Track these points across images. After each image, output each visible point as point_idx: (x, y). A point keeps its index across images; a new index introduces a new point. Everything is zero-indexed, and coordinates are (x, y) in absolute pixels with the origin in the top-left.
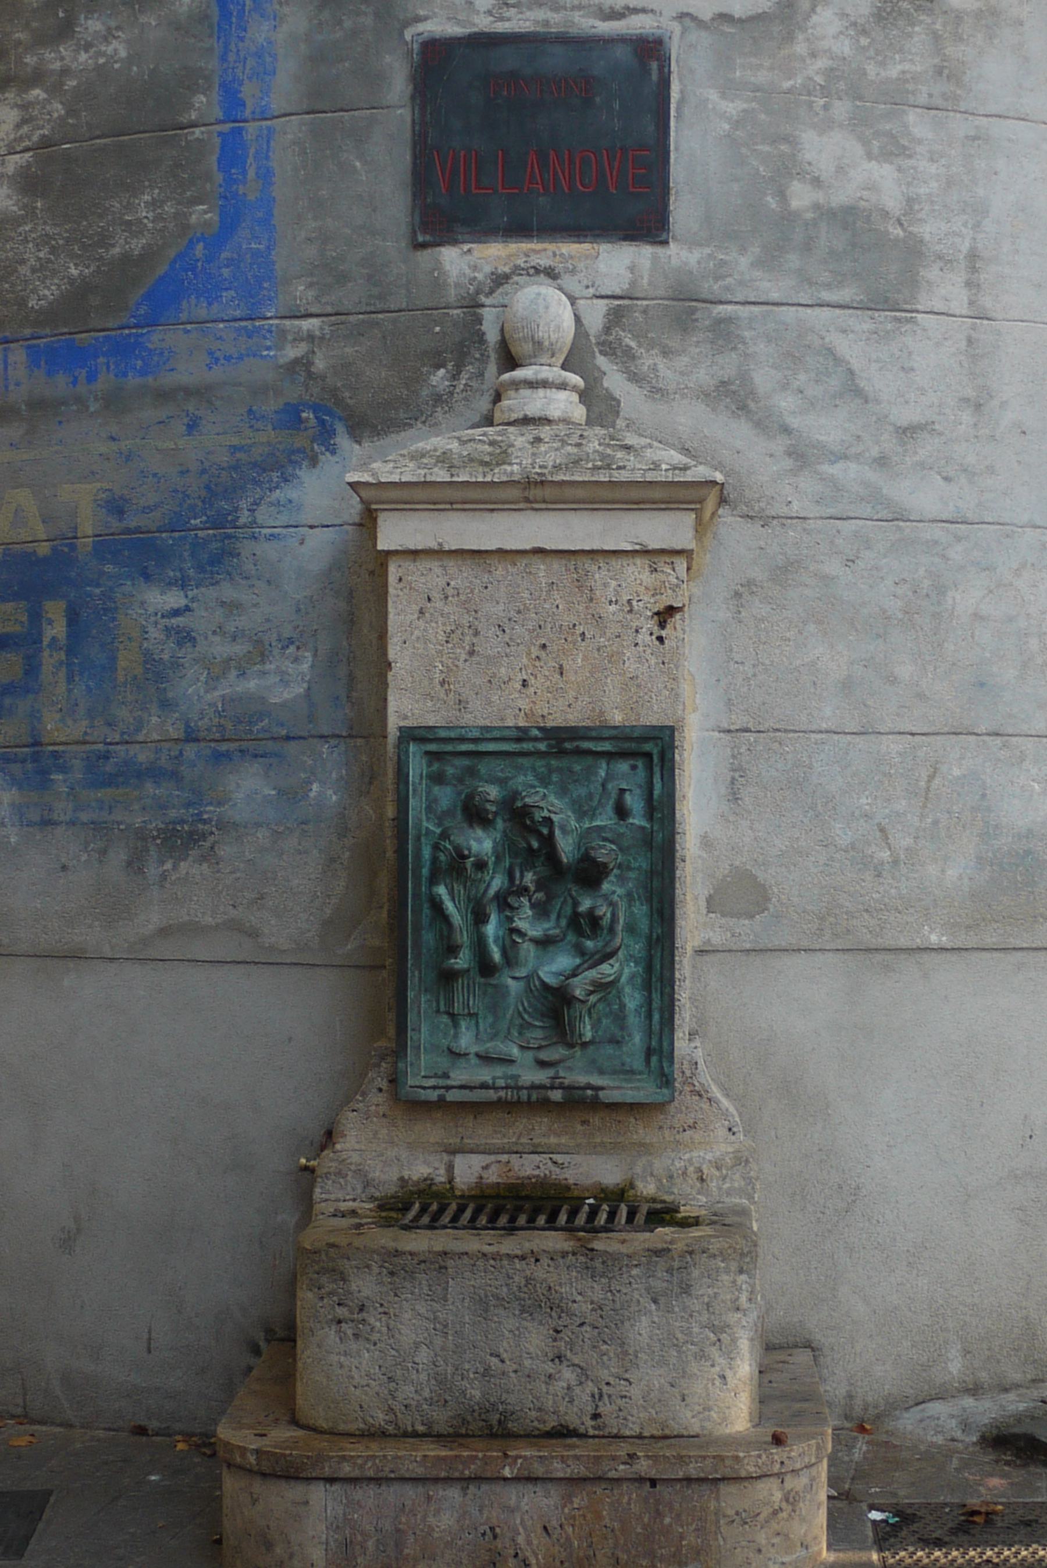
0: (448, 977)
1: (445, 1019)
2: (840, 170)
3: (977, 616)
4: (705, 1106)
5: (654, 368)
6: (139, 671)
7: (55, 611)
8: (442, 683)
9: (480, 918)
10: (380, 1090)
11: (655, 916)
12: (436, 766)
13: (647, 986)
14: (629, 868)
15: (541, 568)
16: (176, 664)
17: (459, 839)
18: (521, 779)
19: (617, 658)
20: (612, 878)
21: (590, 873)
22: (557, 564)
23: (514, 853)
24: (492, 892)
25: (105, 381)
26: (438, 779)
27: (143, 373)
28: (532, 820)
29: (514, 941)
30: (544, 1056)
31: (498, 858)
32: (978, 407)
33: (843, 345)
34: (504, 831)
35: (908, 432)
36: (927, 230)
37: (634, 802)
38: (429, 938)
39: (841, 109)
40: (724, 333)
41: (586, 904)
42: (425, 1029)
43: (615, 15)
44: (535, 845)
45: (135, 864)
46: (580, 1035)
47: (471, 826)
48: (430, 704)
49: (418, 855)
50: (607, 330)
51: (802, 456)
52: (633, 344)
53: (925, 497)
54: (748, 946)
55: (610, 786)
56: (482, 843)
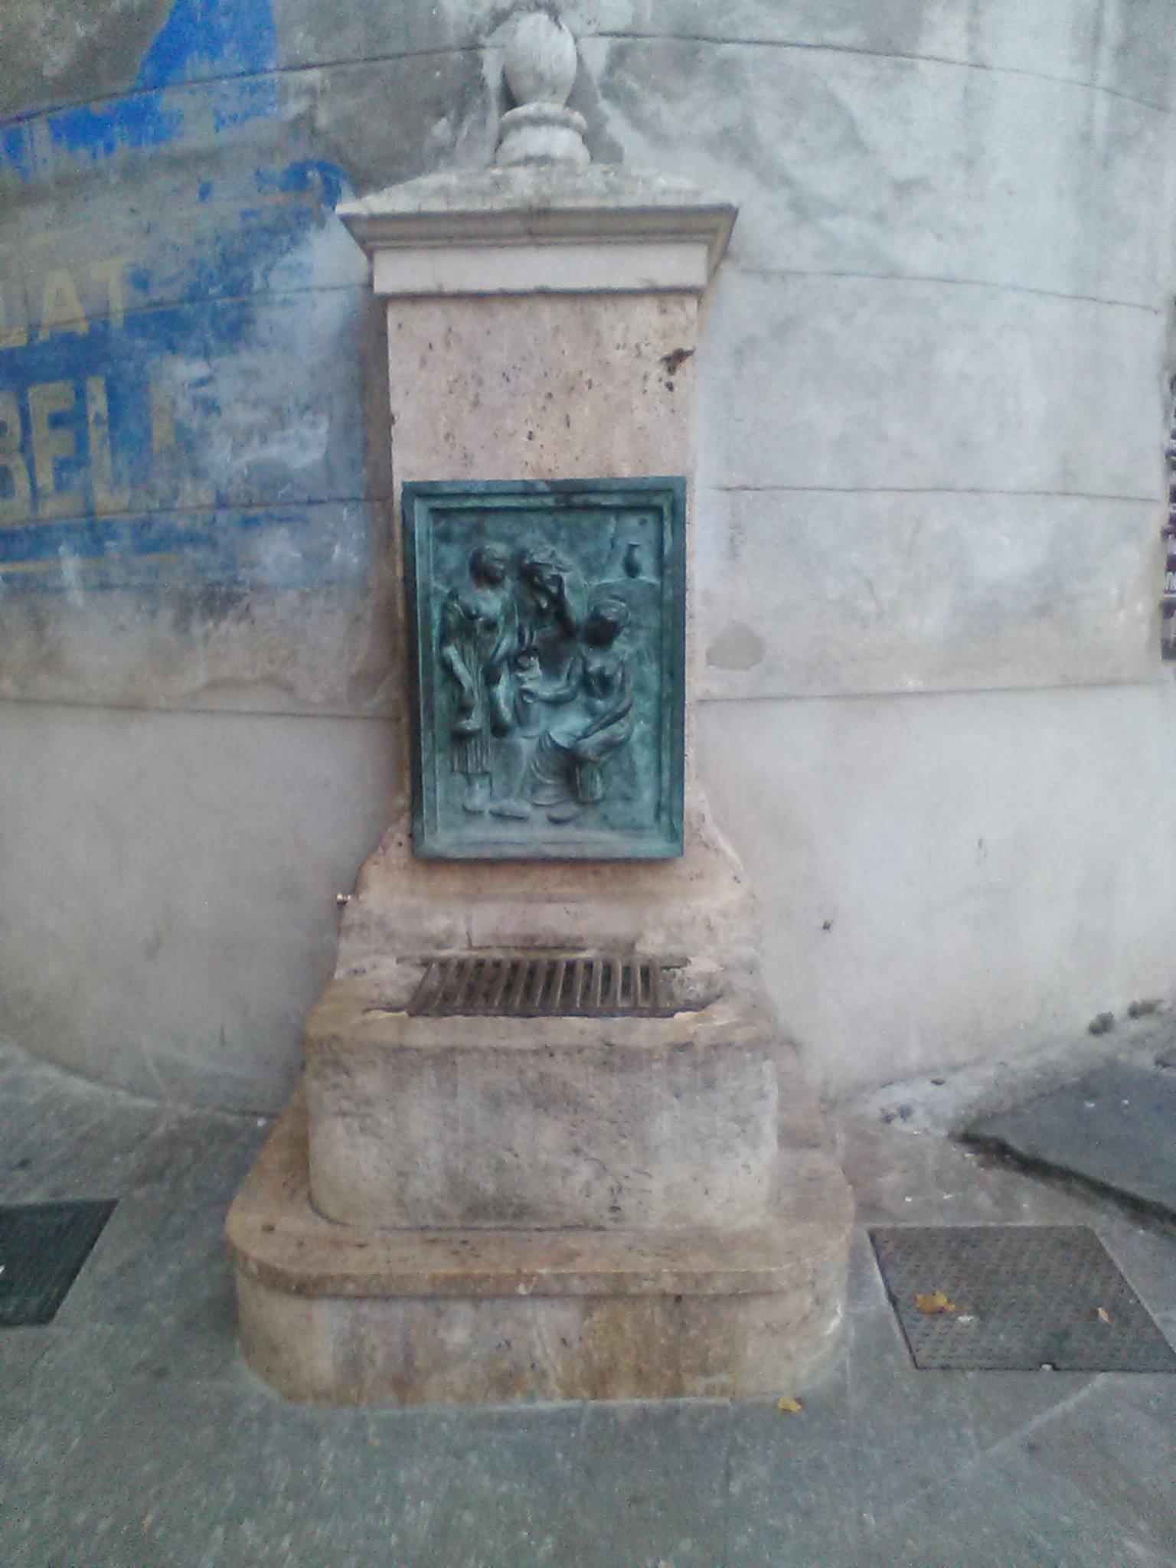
0: (460, 738)
1: (459, 779)
5: (657, 114)
6: (171, 440)
7: (96, 387)
8: (447, 436)
9: (491, 678)
10: (400, 844)
11: (666, 676)
12: (443, 523)
13: (658, 742)
14: (640, 627)
15: (548, 314)
16: (204, 434)
17: (466, 599)
18: (529, 536)
20: (621, 637)
21: (601, 633)
22: (563, 309)
23: (524, 613)
24: (501, 652)
25: (123, 151)
26: (444, 537)
27: (157, 139)
28: (541, 578)
29: (524, 702)
30: (556, 813)
31: (509, 618)
32: (970, 164)
34: (513, 591)
35: (904, 188)
37: (645, 560)
38: (441, 699)
40: (727, 75)
41: (596, 664)
42: (439, 787)
44: (545, 605)
45: (182, 624)
46: (592, 795)
47: (479, 584)
49: (427, 616)
50: (610, 70)
51: (803, 209)
52: (636, 86)
53: (920, 255)
55: (619, 542)
56: (491, 603)
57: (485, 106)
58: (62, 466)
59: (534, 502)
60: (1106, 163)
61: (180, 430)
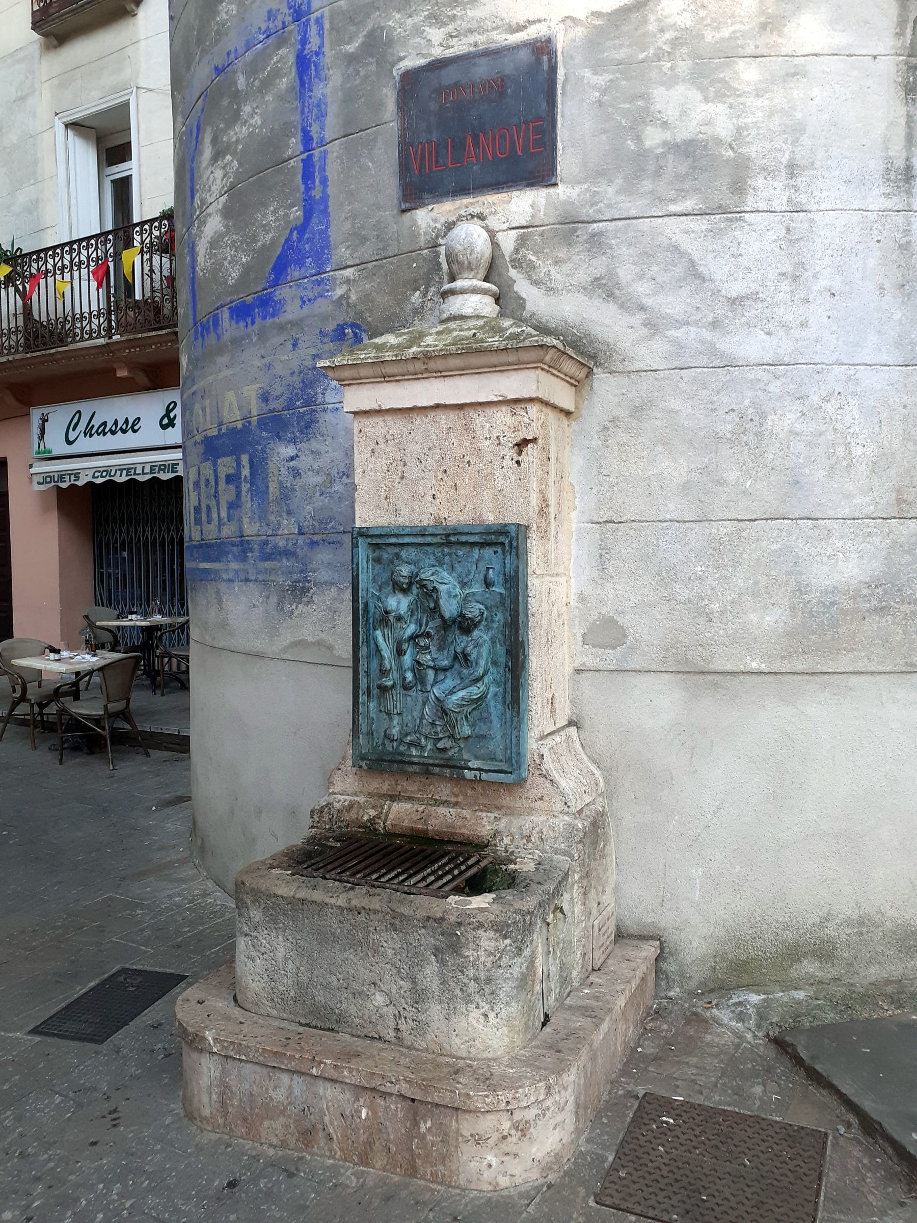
2: (684, 113)
3: (794, 433)
4: (549, 785)
5: (548, 274)
7: (245, 459)
8: (386, 498)
9: (400, 652)
15: (443, 419)
19: (489, 477)
21: (465, 625)
22: (452, 415)
27: (273, 315)
32: (795, 278)
33: (686, 244)
35: (735, 302)
36: (752, 150)
39: (684, 67)
40: (596, 243)
43: (520, 28)
48: (379, 512)
50: (517, 251)
51: (653, 326)
52: (533, 258)
54: (612, 668)
59: (429, 539)
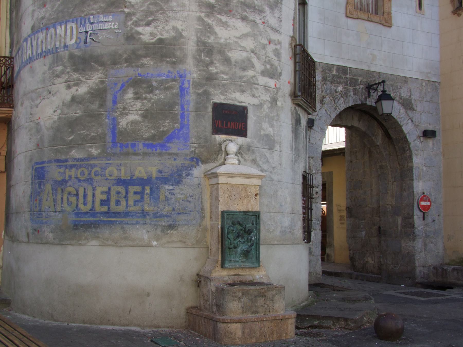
2: (267, 129)
6: (164, 199)
16: (171, 198)
19: (250, 201)
25: (158, 151)
27: (166, 150)
33: (266, 154)
36: (276, 138)
39: (267, 120)
40: (253, 152)
45: (162, 231)
53: (276, 178)
57: (222, 153)
58: (136, 201)
59: (241, 214)
60: (294, 164)
61: (166, 197)
